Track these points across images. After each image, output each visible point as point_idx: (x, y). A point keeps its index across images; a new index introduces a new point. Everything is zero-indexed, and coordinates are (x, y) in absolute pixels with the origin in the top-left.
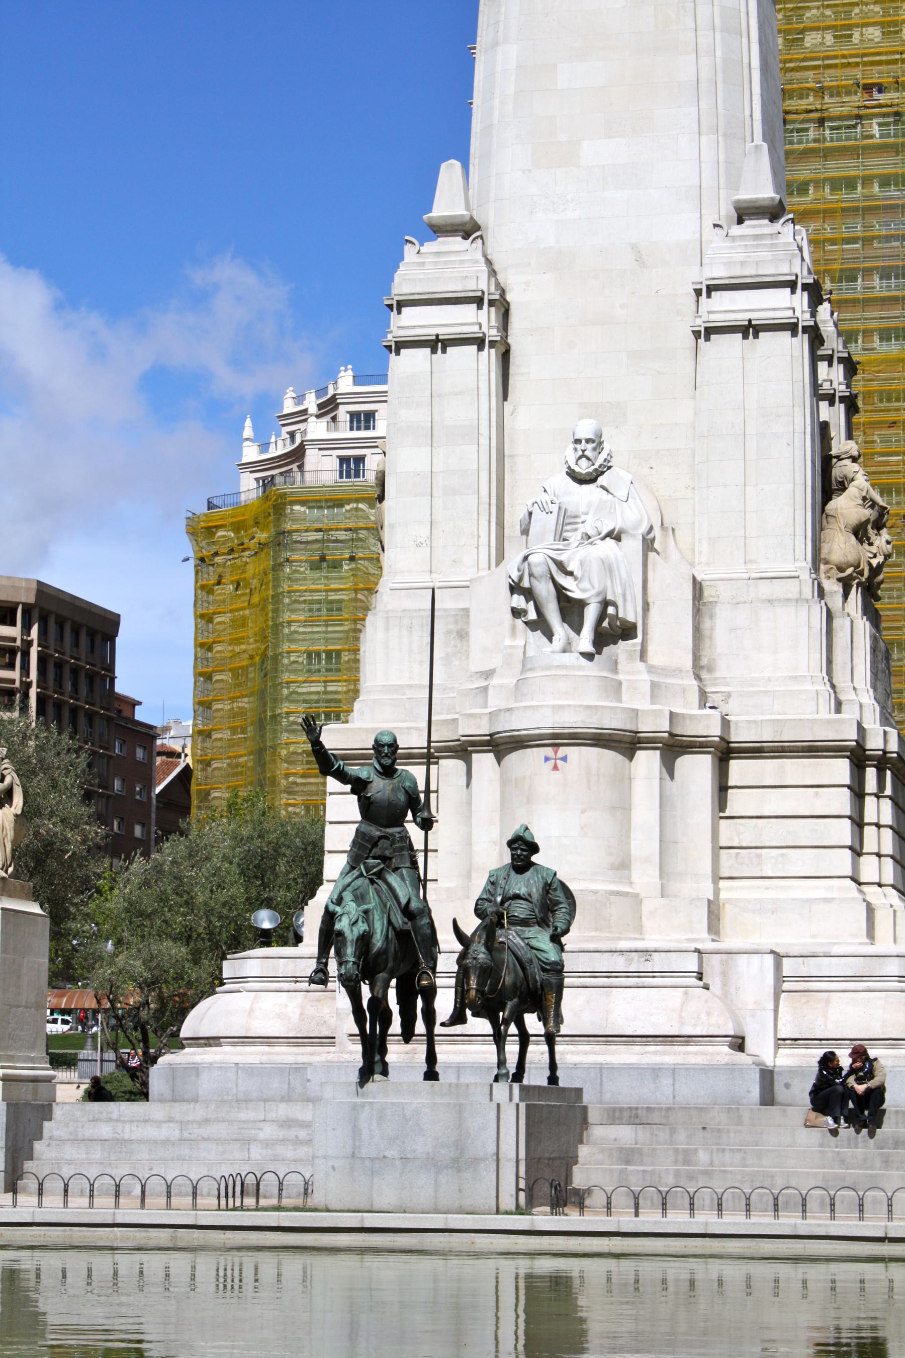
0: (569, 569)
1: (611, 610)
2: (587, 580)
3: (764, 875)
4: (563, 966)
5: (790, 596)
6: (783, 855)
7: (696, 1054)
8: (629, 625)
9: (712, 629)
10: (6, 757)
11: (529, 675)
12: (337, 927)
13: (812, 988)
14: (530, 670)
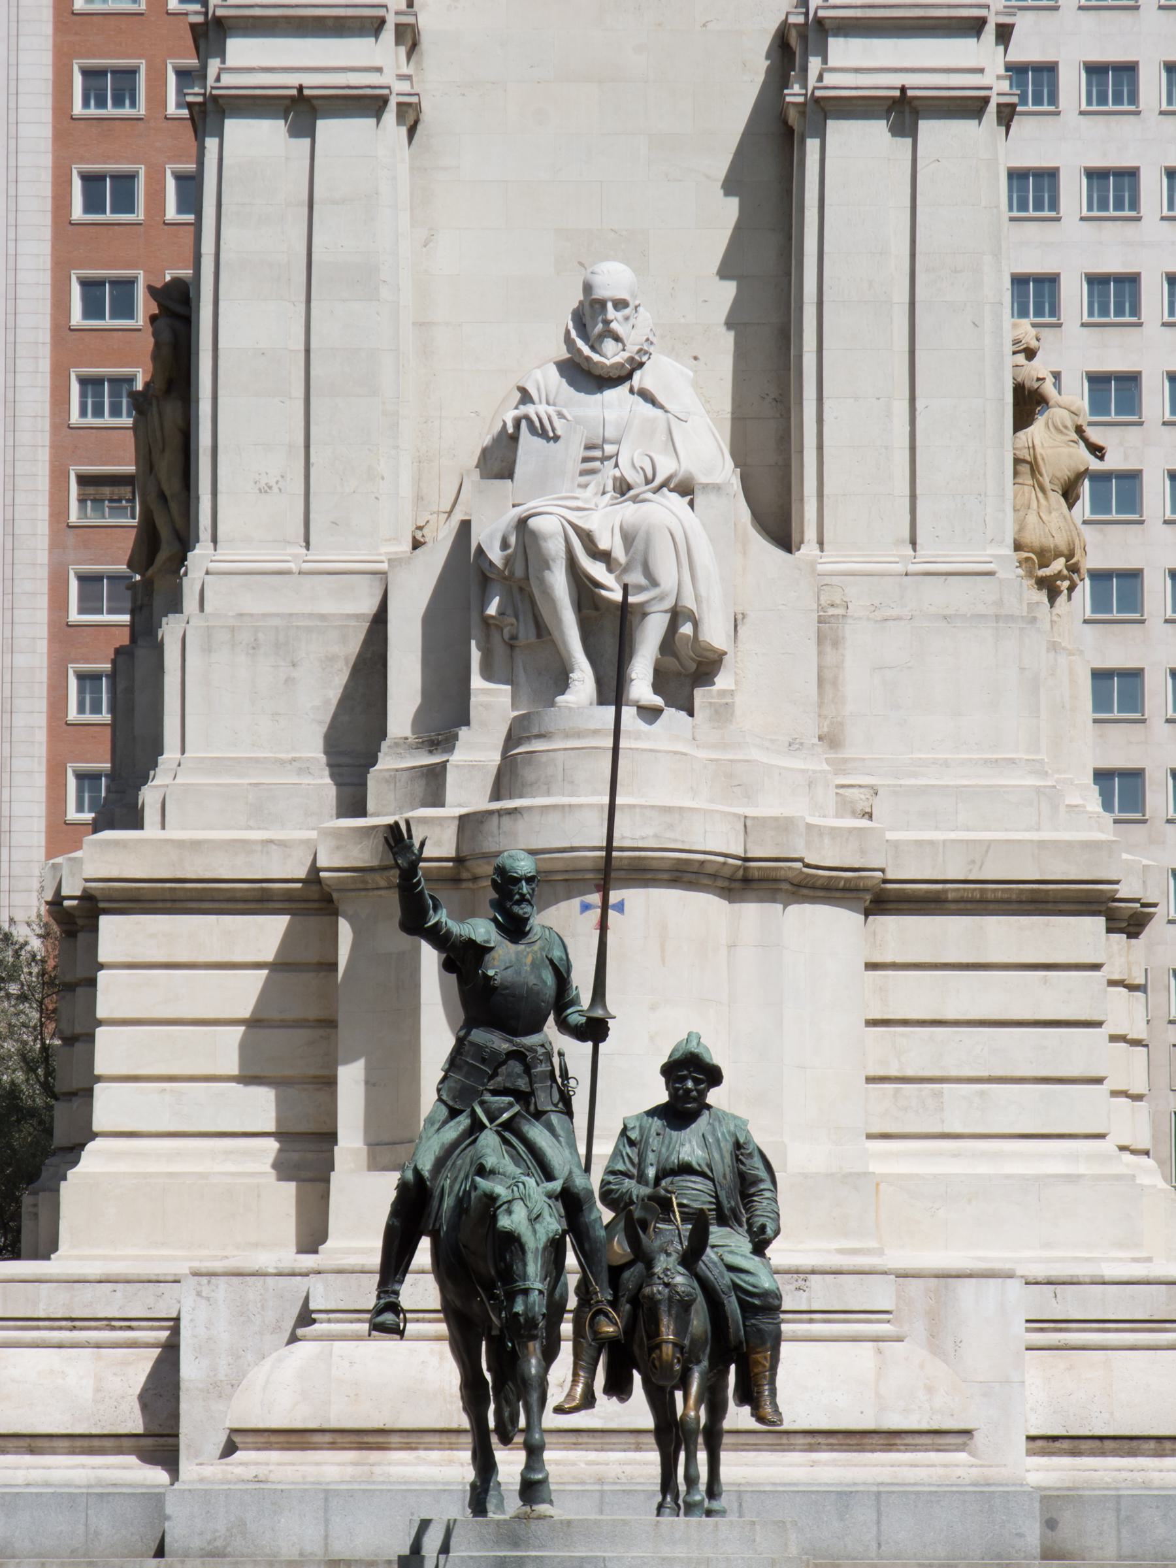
1: (686, 629)
2: (639, 569)
3: (947, 1130)
4: (779, 1298)
6: (982, 1093)
7: (826, 1464)
12: (504, 1222)
13: (1073, 1343)
14: (540, 736)
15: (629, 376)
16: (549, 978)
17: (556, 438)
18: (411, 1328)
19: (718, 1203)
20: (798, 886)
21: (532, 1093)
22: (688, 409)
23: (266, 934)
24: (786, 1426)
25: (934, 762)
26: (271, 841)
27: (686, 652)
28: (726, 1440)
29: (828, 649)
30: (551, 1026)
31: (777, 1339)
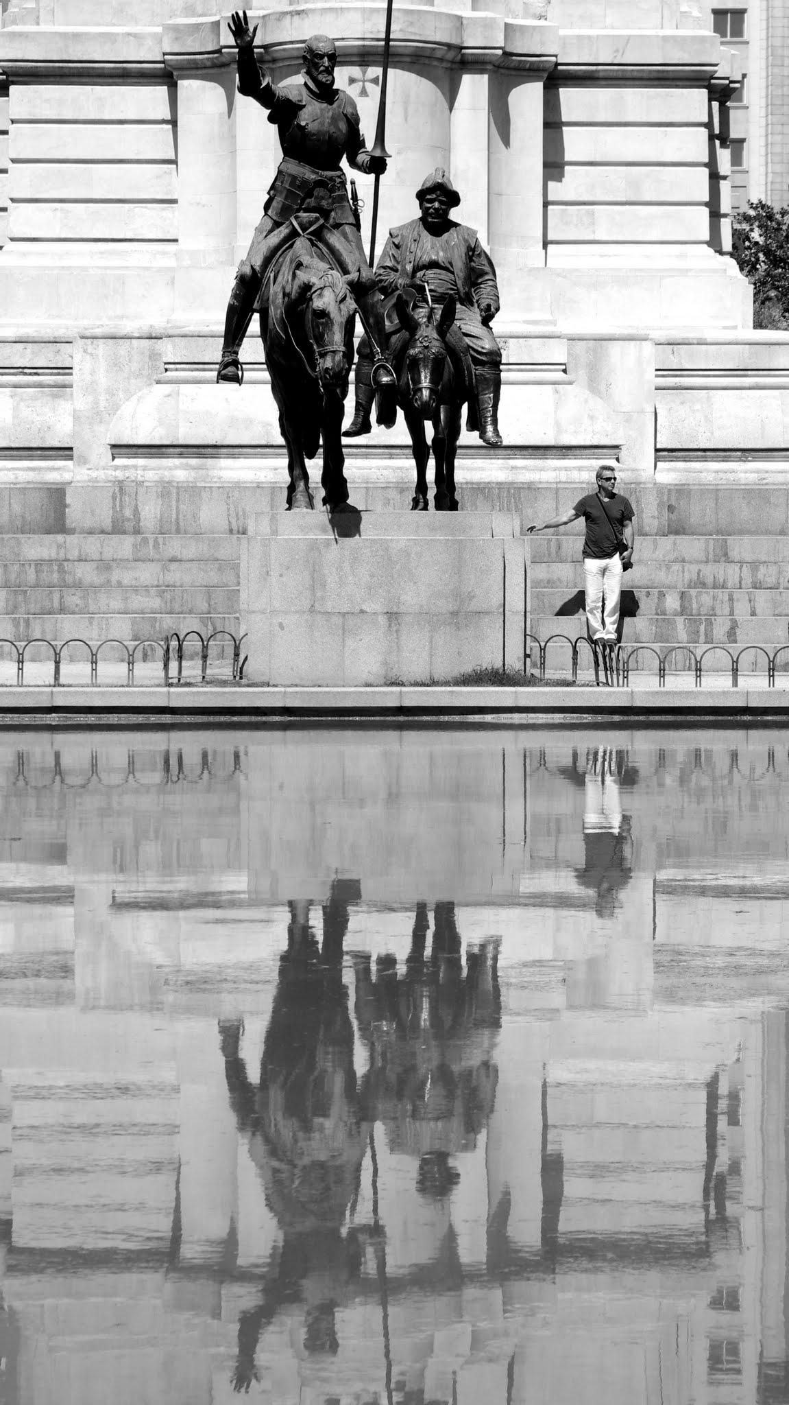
3: (598, 238)
4: (500, 355)
16: (343, 126)
18: (247, 375)
20: (499, 67)
24: (505, 443)
26: (129, 34)
30: (344, 163)
31: (497, 385)
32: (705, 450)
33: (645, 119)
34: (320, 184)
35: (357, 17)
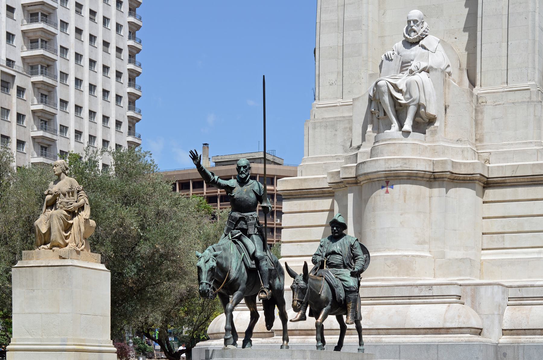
0: (400, 88)
2: (408, 93)
5: (525, 100)
8: (433, 117)
9: (482, 119)
10: (82, 190)
11: (377, 144)
15: (419, 42)
17: (392, 60)
19: (343, 262)
21: (247, 229)
22: (439, 51)
23: (326, 203)
25: (509, 144)
27: (424, 116)
28: (363, 331)
29: (480, 115)
32: (525, 330)
33: (526, 198)
34: (242, 219)
35: (382, 163)
